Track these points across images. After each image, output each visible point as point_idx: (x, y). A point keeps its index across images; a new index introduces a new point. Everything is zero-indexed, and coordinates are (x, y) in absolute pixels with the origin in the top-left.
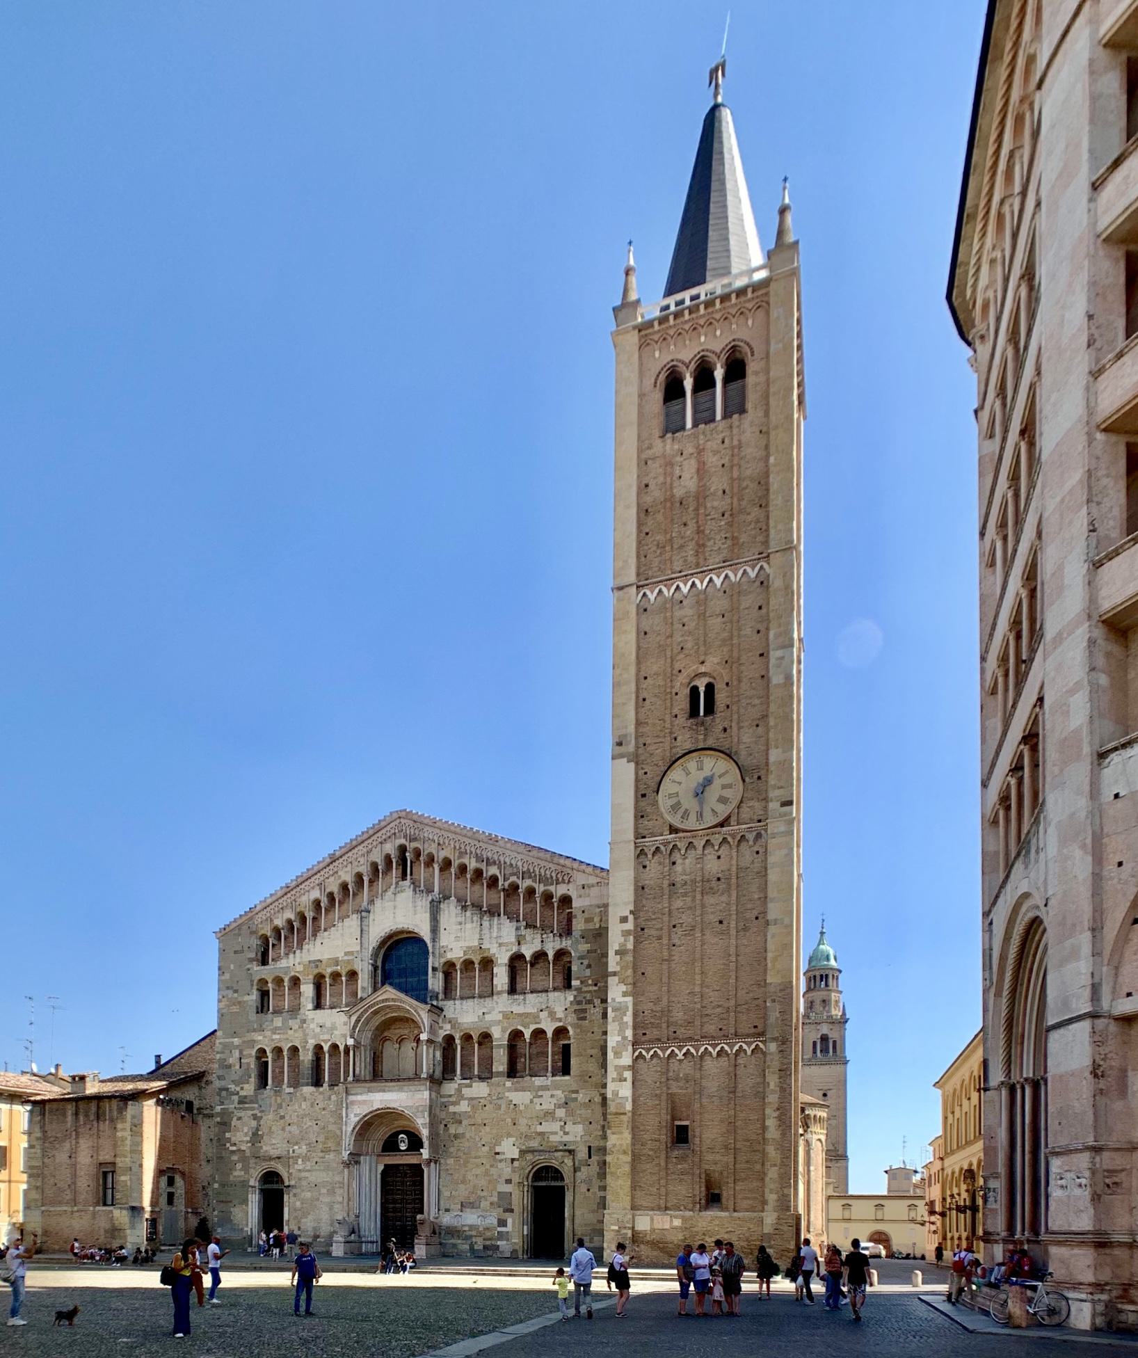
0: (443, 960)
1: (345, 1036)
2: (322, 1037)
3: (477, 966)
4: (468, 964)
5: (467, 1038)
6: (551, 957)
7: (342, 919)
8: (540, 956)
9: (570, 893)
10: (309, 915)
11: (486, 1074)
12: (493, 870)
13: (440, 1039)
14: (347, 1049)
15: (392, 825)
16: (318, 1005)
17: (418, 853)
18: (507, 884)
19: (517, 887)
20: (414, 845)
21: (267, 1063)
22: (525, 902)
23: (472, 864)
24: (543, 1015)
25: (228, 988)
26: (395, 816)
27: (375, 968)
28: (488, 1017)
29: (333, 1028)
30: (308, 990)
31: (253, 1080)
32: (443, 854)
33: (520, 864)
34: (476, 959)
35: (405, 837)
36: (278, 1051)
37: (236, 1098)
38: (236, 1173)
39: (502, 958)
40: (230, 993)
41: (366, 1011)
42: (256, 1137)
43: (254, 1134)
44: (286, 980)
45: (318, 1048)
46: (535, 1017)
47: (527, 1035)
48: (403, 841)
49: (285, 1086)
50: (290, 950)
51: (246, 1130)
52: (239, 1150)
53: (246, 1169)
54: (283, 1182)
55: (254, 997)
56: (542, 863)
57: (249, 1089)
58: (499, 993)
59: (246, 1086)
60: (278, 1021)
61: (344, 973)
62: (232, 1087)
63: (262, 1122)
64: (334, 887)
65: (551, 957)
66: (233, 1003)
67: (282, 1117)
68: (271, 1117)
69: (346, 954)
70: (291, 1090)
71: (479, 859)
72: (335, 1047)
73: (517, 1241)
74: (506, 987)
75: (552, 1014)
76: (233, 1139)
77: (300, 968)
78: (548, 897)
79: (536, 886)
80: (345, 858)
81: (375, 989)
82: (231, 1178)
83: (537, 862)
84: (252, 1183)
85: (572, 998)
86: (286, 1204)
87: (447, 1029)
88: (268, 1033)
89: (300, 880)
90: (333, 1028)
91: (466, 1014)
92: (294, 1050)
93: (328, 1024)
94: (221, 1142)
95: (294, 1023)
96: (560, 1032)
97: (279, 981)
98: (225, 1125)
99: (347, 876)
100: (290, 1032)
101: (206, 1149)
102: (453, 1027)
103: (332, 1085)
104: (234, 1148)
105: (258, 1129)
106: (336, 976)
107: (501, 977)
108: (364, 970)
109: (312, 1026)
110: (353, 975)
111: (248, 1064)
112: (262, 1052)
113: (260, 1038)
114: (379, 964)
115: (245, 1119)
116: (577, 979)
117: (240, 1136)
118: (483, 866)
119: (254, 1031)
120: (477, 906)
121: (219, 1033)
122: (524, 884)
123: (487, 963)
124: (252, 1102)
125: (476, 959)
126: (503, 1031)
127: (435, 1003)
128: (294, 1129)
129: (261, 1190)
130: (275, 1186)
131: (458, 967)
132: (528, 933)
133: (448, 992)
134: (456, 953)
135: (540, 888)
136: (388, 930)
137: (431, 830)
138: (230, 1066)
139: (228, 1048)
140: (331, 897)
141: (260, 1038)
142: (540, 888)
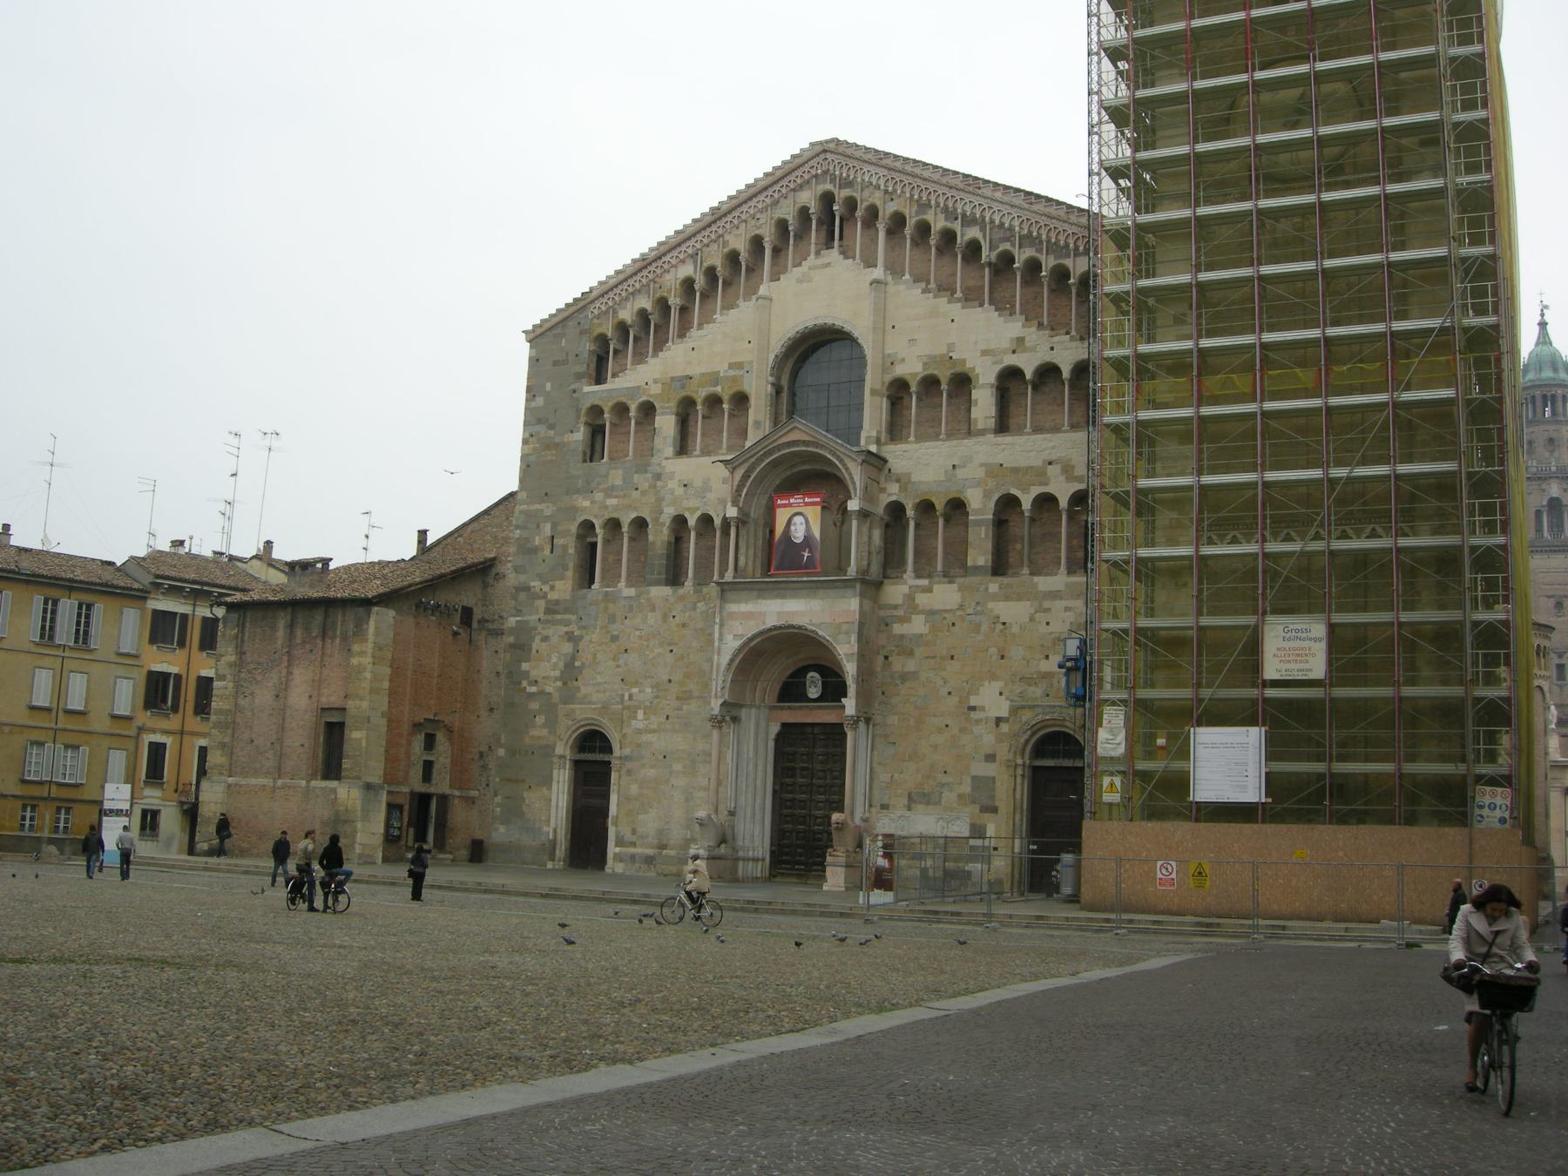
0: (888, 378)
1: (723, 502)
2: (686, 504)
3: (944, 386)
4: (930, 383)
5: (926, 507)
6: (1066, 374)
7: (729, 306)
8: (1048, 372)
10: (675, 301)
11: (956, 565)
12: (973, 233)
13: (880, 510)
14: (726, 522)
15: (811, 163)
16: (683, 449)
17: (851, 204)
19: (1012, 260)
20: (846, 192)
21: (594, 545)
22: (1025, 283)
23: (938, 223)
24: (1053, 471)
25: (539, 421)
26: (820, 148)
27: (778, 390)
28: (960, 473)
29: (706, 488)
30: (666, 423)
31: (570, 574)
32: (892, 207)
33: (1016, 223)
34: (944, 376)
35: (832, 181)
36: (614, 525)
37: (541, 604)
38: (534, 733)
39: (986, 375)
40: (542, 429)
41: (760, 460)
42: (571, 671)
43: (566, 665)
44: (633, 408)
45: (680, 521)
46: (1040, 474)
47: (1026, 503)
48: (829, 187)
49: (622, 584)
50: (640, 357)
51: (554, 660)
52: (542, 692)
53: (551, 723)
54: (608, 749)
55: (580, 435)
56: (1053, 224)
57: (563, 588)
58: (982, 432)
59: (559, 584)
60: (616, 477)
61: (726, 398)
62: (536, 584)
63: (582, 645)
64: (716, 258)
65: (1066, 374)
66: (549, 445)
67: (614, 639)
68: (595, 637)
69: (731, 366)
70: (631, 592)
71: (950, 214)
72: (706, 520)
73: (1000, 865)
74: (992, 423)
77: (656, 389)
78: (1061, 274)
79: (1043, 258)
80: (736, 213)
81: (776, 421)
82: (527, 740)
83: (1043, 221)
84: (559, 750)
86: (613, 787)
87: (893, 492)
88: (599, 496)
89: (663, 249)
90: (706, 488)
91: (925, 464)
92: (640, 524)
93: (698, 483)
94: (514, 677)
96: (1080, 499)
97: (621, 409)
98: (521, 649)
99: (739, 242)
100: (636, 494)
102: (903, 489)
103: (701, 581)
104: (534, 689)
105: (573, 658)
106: (714, 401)
107: (984, 403)
108: (759, 388)
109: (672, 484)
110: (741, 400)
111: (565, 547)
112: (588, 526)
113: (587, 503)
114: (785, 382)
115: (555, 639)
117: (544, 669)
118: (957, 226)
119: (578, 492)
120: (946, 288)
121: (519, 496)
122: (1021, 256)
123: (963, 382)
124: (567, 611)
125: (944, 376)
126: (987, 495)
127: (873, 448)
128: (632, 658)
129: (577, 764)
130: (598, 757)
131: (913, 389)
132: (1032, 335)
133: (895, 430)
134: (912, 368)
135: (1048, 263)
136: (800, 327)
137: (873, 169)
138: (534, 551)
139: (534, 520)
140: (711, 273)
141: (587, 503)
142: (1048, 263)
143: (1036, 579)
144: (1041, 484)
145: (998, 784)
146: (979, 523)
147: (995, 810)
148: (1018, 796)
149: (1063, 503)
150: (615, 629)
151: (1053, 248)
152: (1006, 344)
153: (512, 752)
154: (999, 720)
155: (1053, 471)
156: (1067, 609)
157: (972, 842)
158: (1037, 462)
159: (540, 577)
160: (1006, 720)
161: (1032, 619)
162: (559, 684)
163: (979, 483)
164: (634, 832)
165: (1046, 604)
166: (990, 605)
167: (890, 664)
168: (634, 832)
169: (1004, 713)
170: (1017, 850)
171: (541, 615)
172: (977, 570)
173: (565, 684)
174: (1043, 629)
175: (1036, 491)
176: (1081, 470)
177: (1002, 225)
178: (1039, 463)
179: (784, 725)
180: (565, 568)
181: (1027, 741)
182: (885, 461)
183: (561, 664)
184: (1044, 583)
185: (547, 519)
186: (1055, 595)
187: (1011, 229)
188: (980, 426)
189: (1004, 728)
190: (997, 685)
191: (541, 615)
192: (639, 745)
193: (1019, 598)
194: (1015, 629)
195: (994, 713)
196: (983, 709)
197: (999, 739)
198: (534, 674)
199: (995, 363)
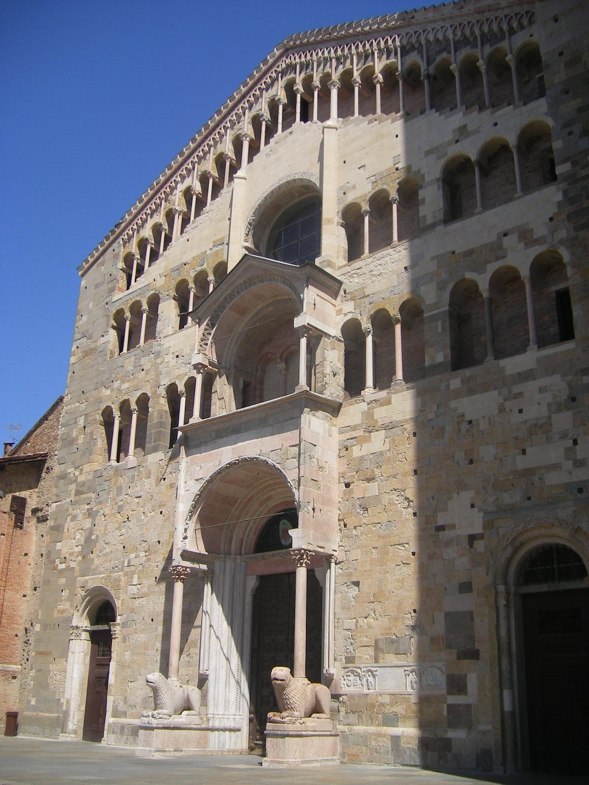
9: (535, 39)
18: (432, 69)
37: (73, 487)
45: (172, 390)
46: (496, 250)
47: (483, 282)
52: (68, 568)
75: (526, 236)
76: (64, 550)
77: (161, 282)
79: (477, 52)
82: (56, 614)
85: (559, 197)
88: (116, 384)
92: (143, 401)
95: (146, 362)
101: (31, 570)
104: (63, 566)
105: (91, 532)
113: (108, 392)
115: (80, 517)
116: (564, 161)
126: (441, 287)
134: (361, 191)
143: (503, 362)
144: (498, 259)
145: (477, 620)
146: (433, 318)
147: (475, 655)
148: (503, 633)
149: (525, 272)
151: (486, 39)
152: (449, 137)
153: (45, 627)
154: (472, 538)
156: (541, 390)
157: (452, 700)
158: (491, 237)
160: (481, 536)
161: (502, 409)
162: (80, 558)
164: (125, 700)
165: (516, 389)
166: (453, 404)
167: (352, 492)
168: (125, 700)
169: (478, 529)
170: (507, 707)
171: (72, 498)
172: (436, 369)
173: (84, 557)
174: (516, 418)
175: (492, 267)
176: (541, 231)
177: (437, 40)
178: (493, 238)
179: (262, 579)
181: (509, 561)
182: (340, 283)
183: (83, 539)
184: (513, 364)
186: (527, 376)
187: (446, 39)
188: (429, 221)
189: (479, 545)
190: (467, 496)
191: (72, 498)
192: (133, 611)
193: (485, 388)
194: (483, 425)
196: (453, 527)
198: (65, 552)
199: (438, 158)
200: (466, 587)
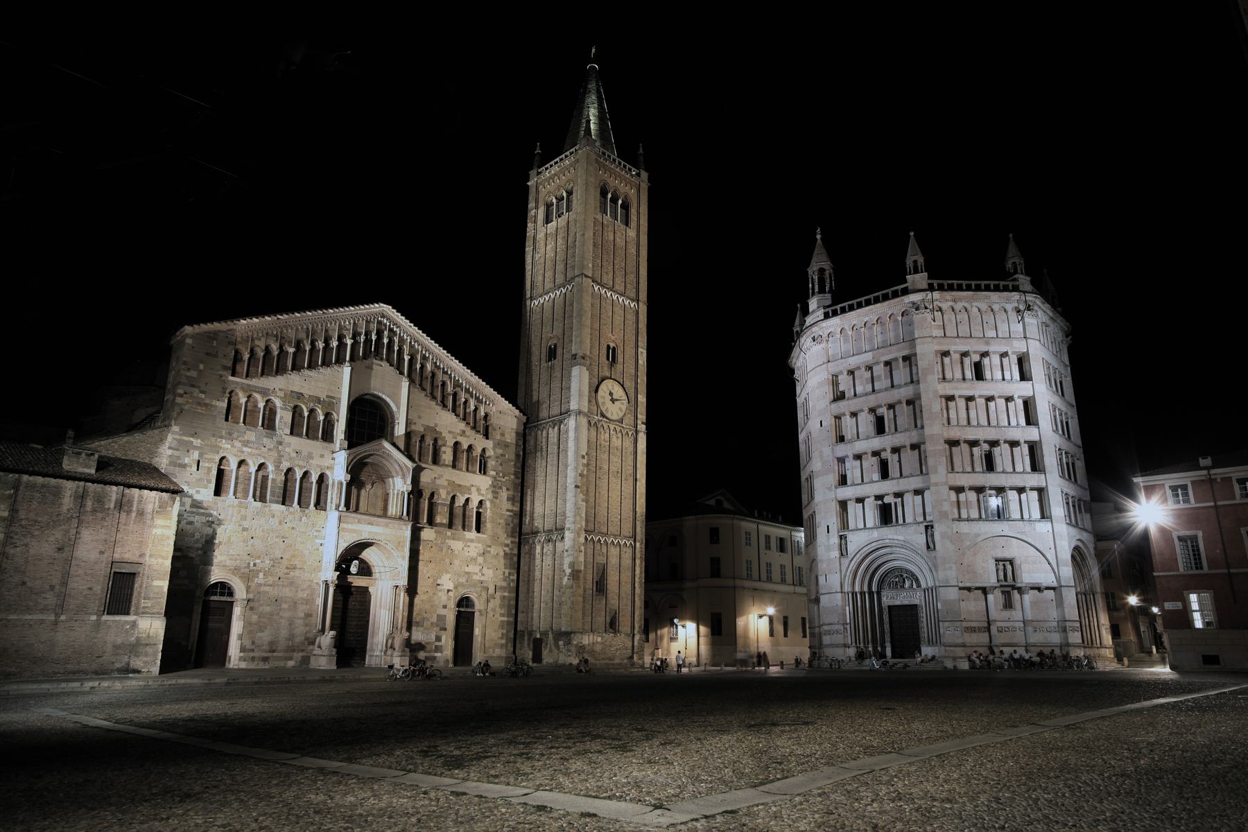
28: (438, 482)
31: (213, 486)
67: (245, 529)
88: (238, 444)
93: (305, 453)
100: (265, 450)
119: (221, 437)
126: (448, 493)
150: (246, 524)
155: (474, 489)
159: (188, 483)
163: (445, 488)
172: (441, 525)
180: (209, 482)
185: (196, 448)
186: (472, 541)
195: (446, 588)
197: (449, 599)
200: (445, 607)
